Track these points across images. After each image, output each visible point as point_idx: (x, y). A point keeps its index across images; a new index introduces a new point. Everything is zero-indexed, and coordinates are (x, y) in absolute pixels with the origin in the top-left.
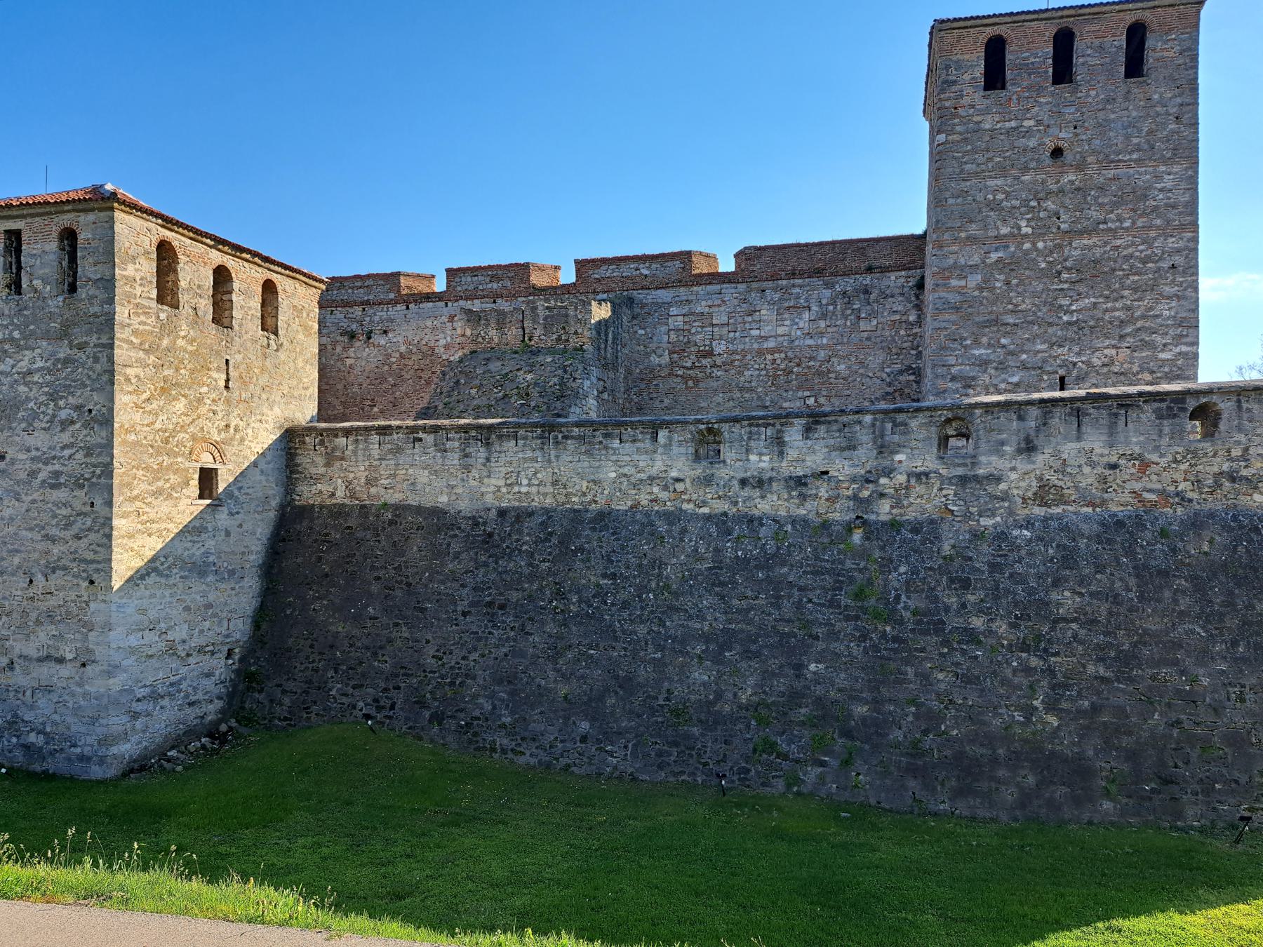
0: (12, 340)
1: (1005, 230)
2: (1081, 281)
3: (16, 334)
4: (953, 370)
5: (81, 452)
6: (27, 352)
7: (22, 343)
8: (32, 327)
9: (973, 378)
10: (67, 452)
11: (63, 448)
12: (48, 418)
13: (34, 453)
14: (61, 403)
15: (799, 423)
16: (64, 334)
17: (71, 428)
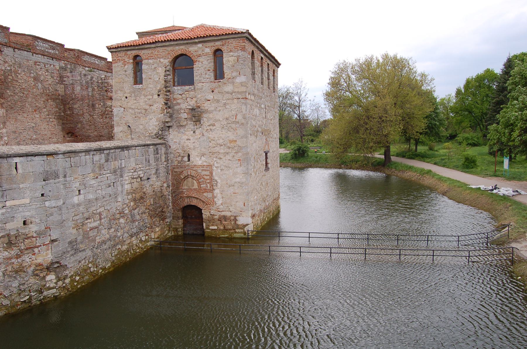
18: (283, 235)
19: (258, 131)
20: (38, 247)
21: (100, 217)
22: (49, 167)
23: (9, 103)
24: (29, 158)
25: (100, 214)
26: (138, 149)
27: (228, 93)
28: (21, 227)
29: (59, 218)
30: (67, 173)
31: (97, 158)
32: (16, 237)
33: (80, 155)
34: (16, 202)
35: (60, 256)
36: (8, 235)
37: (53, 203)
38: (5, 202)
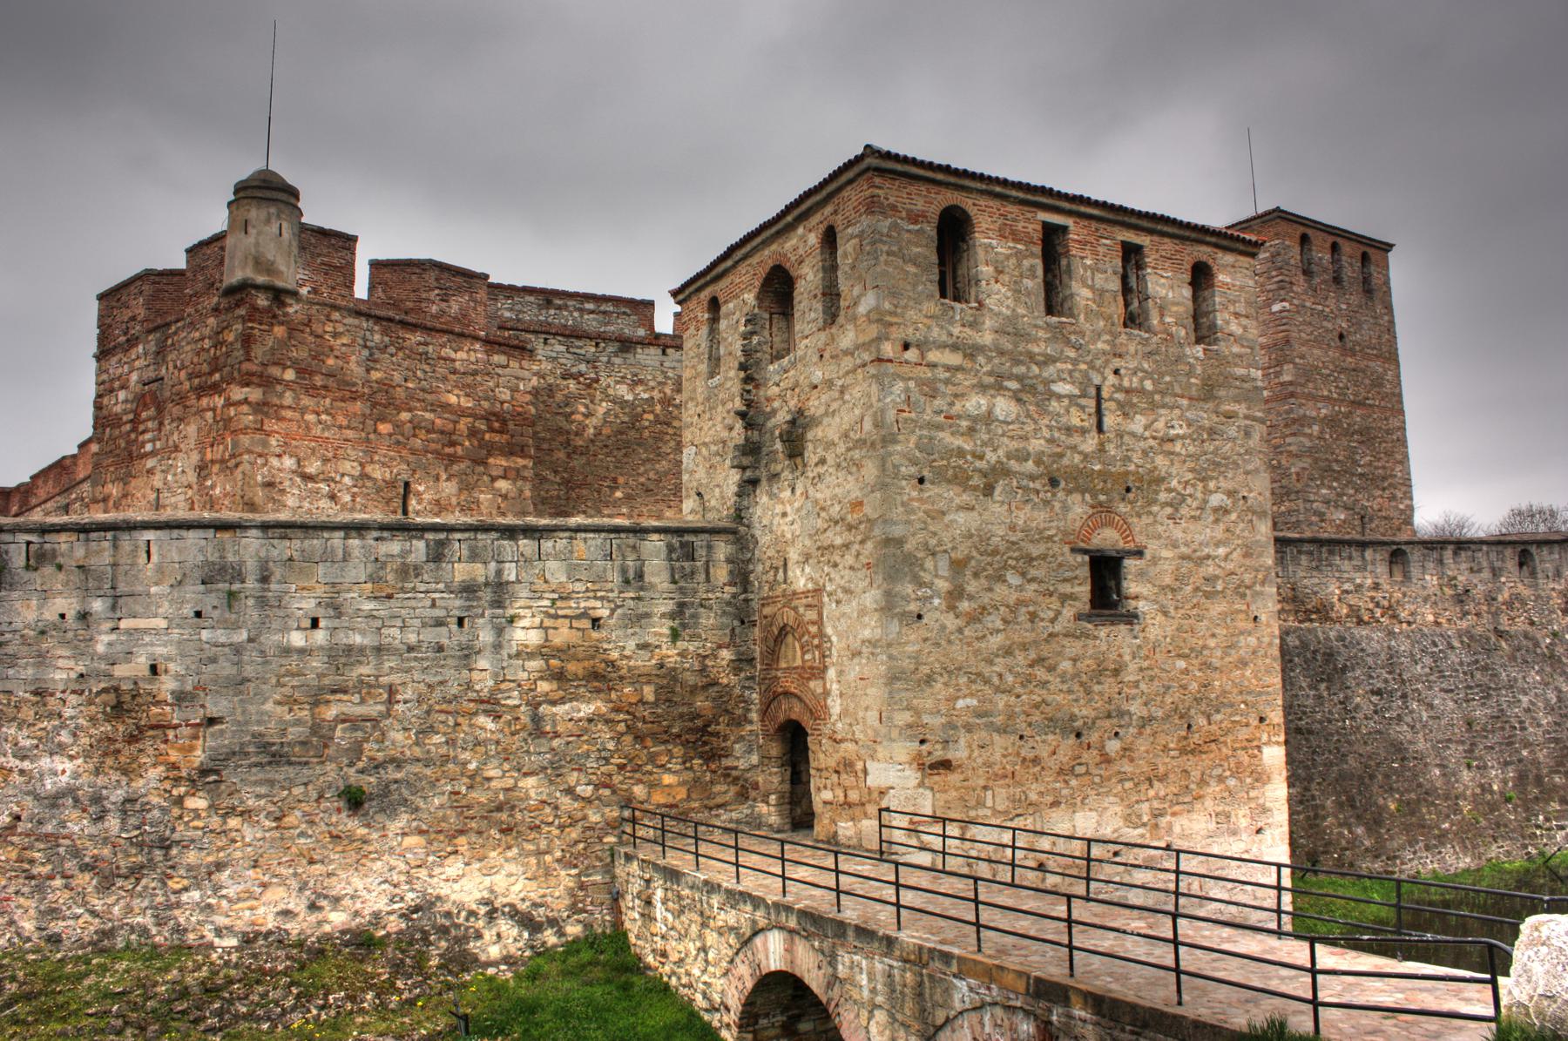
0: (1141, 391)
1: (1326, 393)
2: (1362, 442)
3: (1148, 385)
4: (1315, 505)
5: (1238, 550)
6: (1162, 411)
7: (1157, 397)
8: (1167, 379)
9: (1324, 514)
10: (1222, 551)
11: (1217, 545)
12: (1195, 505)
13: (1184, 549)
14: (1212, 485)
15: (1451, 547)
16: (1208, 393)
17: (1225, 519)
18: (894, 824)
19: (1000, 471)
20: (175, 727)
21: (390, 696)
22: (217, 555)
23: (642, 480)
24: (175, 533)
25: (391, 690)
26: (585, 539)
27: (847, 353)
28: (144, 679)
29: (232, 671)
30: (272, 574)
31: (394, 547)
32: (134, 697)
33: (326, 535)
34: (141, 623)
35: (221, 757)
36: (116, 689)
37: (221, 636)
38: (119, 619)
